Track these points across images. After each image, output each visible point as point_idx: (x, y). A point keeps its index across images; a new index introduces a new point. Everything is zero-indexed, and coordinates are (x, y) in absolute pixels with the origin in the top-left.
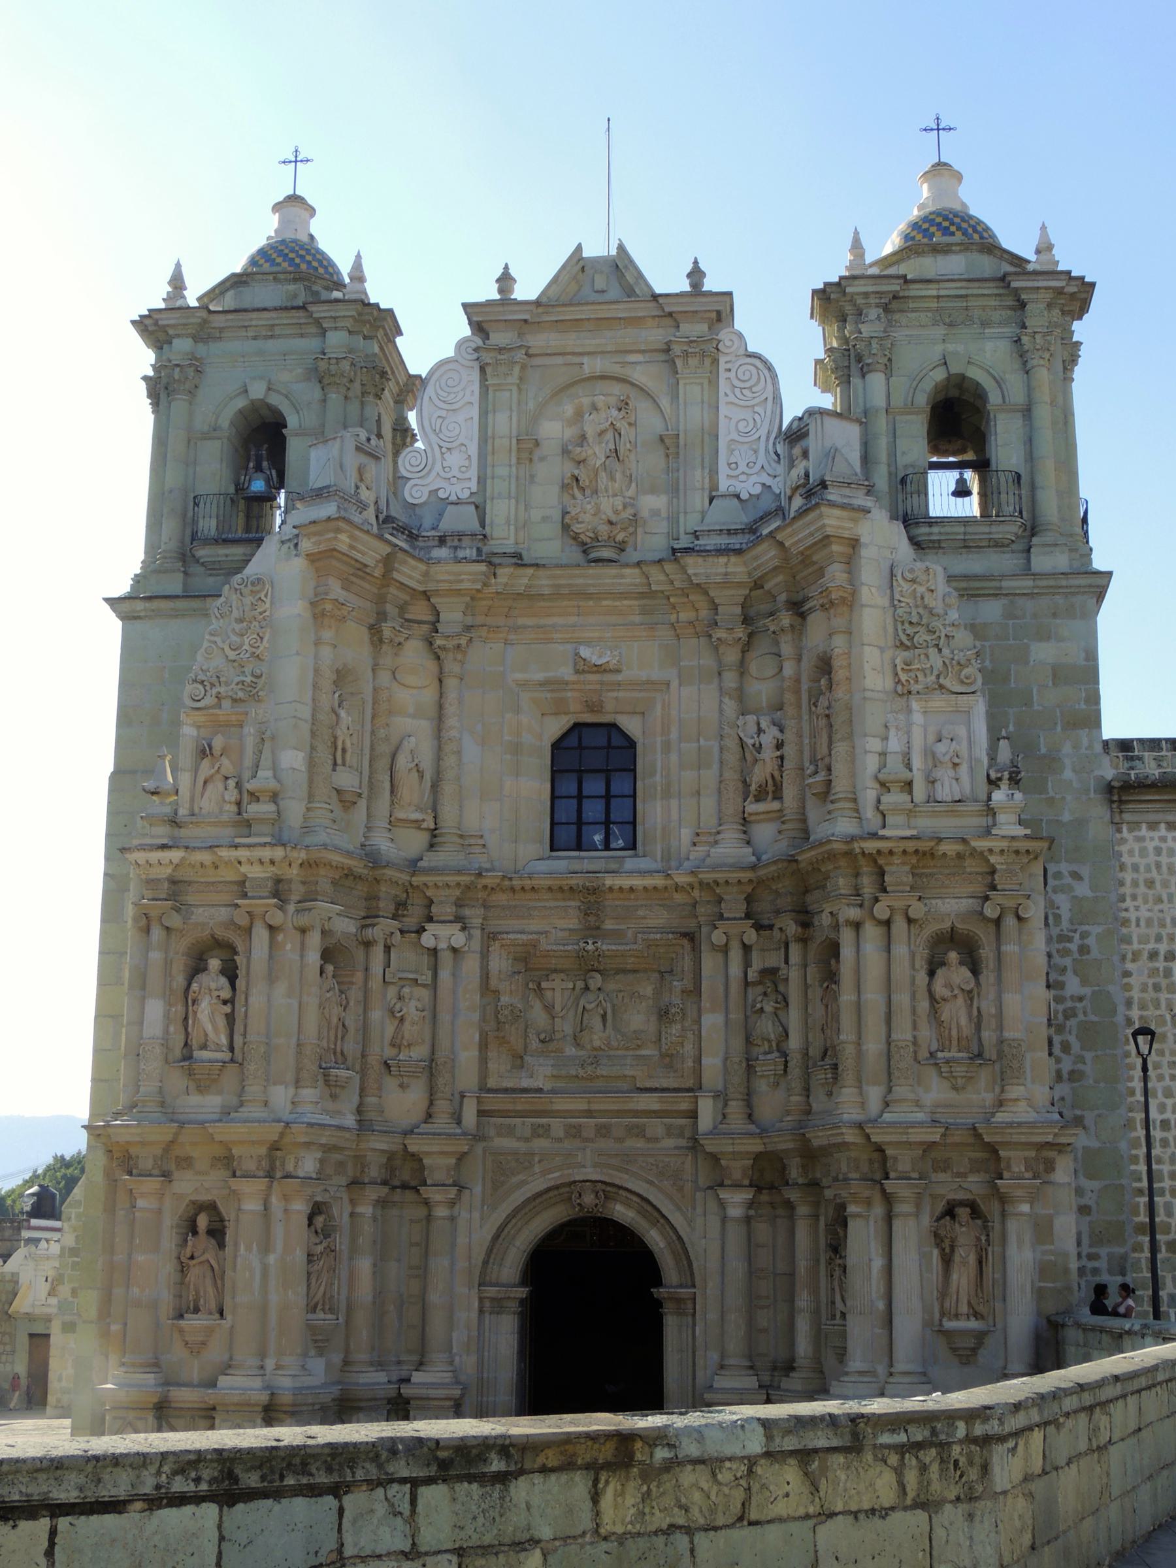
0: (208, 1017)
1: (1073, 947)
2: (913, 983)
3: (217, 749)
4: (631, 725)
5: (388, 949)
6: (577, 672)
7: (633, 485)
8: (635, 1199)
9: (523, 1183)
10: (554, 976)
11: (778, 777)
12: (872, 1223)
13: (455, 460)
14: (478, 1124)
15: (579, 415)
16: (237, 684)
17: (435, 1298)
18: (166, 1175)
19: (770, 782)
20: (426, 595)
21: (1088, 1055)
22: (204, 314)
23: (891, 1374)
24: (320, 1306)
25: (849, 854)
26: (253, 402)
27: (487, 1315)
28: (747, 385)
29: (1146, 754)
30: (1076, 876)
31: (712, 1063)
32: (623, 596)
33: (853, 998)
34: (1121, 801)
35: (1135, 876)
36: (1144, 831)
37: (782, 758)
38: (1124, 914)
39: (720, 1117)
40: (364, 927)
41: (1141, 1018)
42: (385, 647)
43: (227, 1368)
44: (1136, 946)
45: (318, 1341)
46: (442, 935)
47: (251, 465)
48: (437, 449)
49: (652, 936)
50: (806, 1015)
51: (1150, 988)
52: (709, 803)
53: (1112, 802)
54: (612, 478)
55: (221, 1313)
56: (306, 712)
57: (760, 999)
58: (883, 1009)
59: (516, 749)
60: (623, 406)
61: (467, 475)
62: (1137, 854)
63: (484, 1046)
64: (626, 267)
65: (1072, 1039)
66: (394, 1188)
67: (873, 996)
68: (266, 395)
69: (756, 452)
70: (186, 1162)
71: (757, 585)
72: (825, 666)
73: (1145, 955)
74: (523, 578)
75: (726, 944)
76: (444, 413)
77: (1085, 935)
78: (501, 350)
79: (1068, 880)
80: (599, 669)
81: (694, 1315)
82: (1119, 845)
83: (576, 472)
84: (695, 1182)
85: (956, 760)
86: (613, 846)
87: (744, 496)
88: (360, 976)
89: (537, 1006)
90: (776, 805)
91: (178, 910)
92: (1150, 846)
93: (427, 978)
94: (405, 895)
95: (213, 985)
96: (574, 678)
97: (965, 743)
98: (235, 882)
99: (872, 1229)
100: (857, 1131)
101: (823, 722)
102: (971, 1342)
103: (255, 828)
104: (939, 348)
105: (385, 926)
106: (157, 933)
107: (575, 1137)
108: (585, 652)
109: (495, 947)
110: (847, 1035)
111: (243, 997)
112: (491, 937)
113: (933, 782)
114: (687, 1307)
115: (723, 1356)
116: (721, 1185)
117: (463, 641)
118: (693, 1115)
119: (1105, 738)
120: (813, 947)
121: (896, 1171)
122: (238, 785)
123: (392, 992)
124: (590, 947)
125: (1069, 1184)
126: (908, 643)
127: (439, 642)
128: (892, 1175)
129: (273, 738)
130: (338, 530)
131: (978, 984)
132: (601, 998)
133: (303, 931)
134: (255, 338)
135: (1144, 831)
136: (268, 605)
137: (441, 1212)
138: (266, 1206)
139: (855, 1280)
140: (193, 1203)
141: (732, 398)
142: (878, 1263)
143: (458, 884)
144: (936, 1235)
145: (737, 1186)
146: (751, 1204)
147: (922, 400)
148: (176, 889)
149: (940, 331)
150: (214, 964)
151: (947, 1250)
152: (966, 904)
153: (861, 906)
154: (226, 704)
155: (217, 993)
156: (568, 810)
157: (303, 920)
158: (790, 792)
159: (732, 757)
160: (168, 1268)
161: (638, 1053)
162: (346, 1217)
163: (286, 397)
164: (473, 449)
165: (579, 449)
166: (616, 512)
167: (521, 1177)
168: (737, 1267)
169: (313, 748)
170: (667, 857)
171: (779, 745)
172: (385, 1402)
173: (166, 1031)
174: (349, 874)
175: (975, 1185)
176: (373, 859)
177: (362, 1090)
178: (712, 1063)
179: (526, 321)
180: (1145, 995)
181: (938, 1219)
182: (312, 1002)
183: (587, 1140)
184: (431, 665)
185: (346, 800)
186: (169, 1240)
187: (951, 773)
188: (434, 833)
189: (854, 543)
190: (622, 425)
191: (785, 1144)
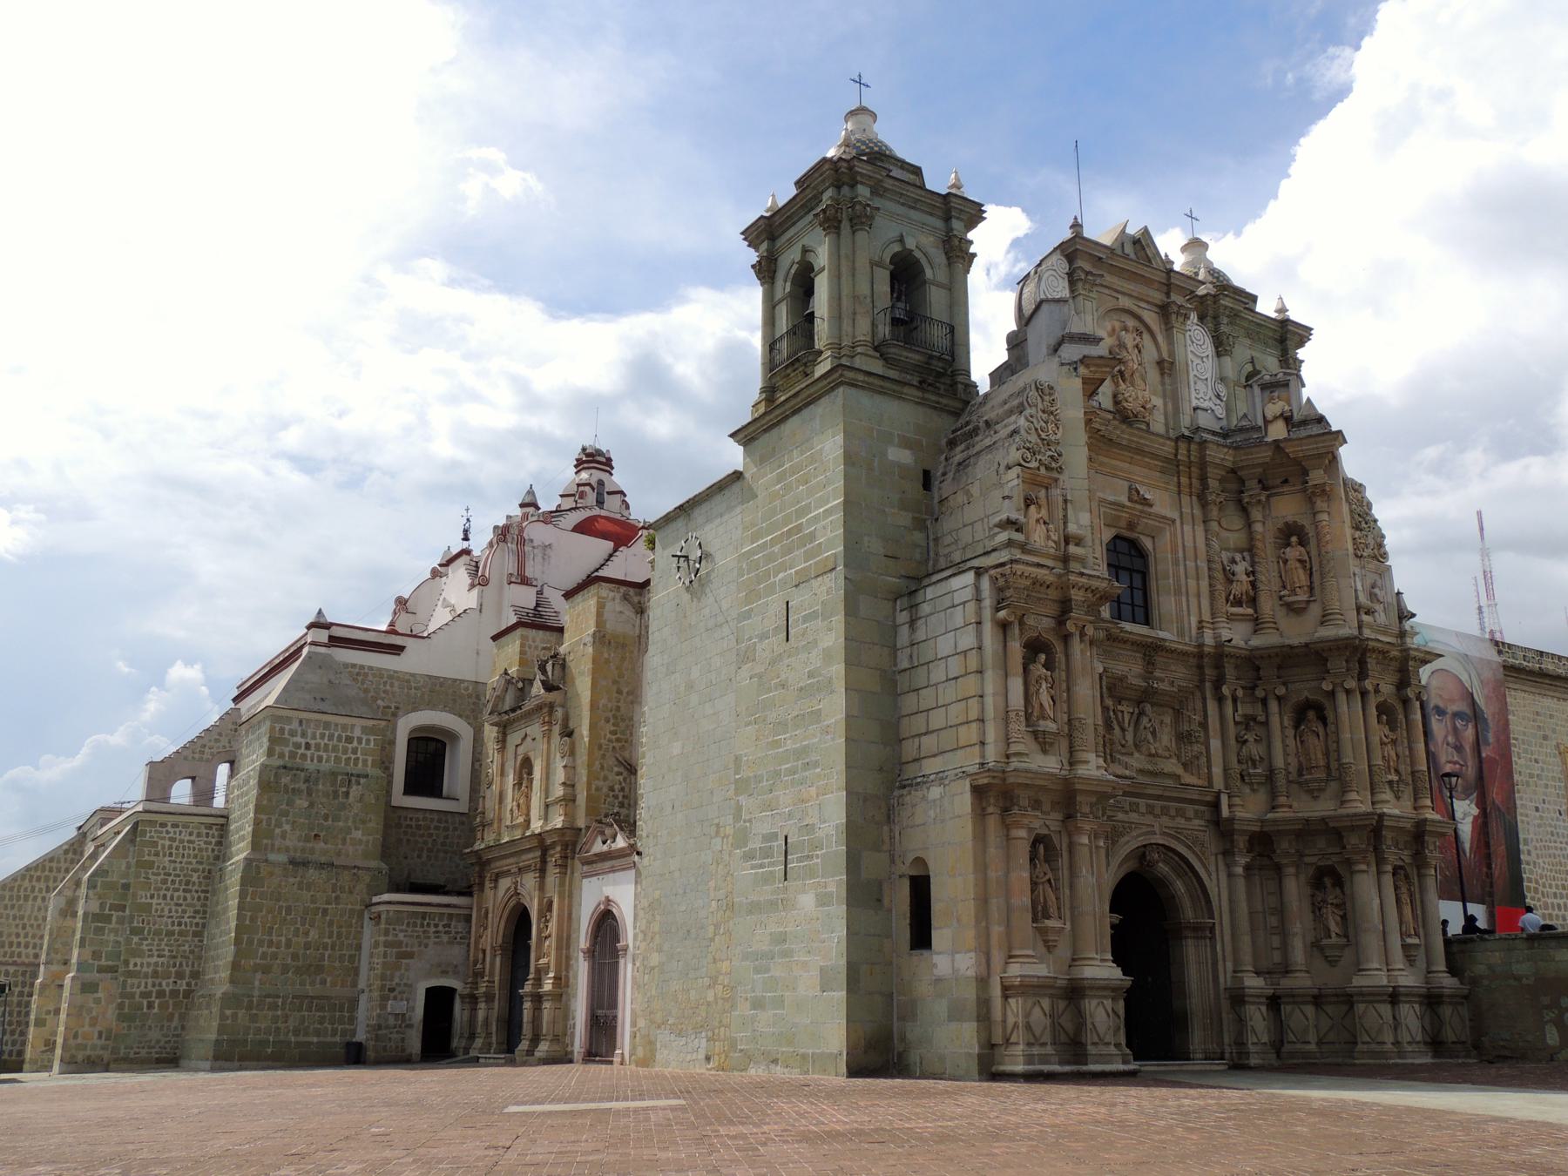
4: (1147, 543)
6: (1130, 500)
25: (1356, 648)
26: (905, 249)
31: (1217, 771)
32: (1154, 456)
50: (1285, 746)
71: (1233, 471)
78: (1087, 273)
80: (1145, 502)
81: (1212, 938)
90: (1250, 611)
104: (1248, 353)
110: (1347, 758)
114: (1206, 932)
115: (1236, 961)
146: (1247, 868)
150: (1043, 657)
154: (1043, 470)
158: (1267, 605)
159: (1219, 575)
168: (1243, 907)
178: (1217, 771)
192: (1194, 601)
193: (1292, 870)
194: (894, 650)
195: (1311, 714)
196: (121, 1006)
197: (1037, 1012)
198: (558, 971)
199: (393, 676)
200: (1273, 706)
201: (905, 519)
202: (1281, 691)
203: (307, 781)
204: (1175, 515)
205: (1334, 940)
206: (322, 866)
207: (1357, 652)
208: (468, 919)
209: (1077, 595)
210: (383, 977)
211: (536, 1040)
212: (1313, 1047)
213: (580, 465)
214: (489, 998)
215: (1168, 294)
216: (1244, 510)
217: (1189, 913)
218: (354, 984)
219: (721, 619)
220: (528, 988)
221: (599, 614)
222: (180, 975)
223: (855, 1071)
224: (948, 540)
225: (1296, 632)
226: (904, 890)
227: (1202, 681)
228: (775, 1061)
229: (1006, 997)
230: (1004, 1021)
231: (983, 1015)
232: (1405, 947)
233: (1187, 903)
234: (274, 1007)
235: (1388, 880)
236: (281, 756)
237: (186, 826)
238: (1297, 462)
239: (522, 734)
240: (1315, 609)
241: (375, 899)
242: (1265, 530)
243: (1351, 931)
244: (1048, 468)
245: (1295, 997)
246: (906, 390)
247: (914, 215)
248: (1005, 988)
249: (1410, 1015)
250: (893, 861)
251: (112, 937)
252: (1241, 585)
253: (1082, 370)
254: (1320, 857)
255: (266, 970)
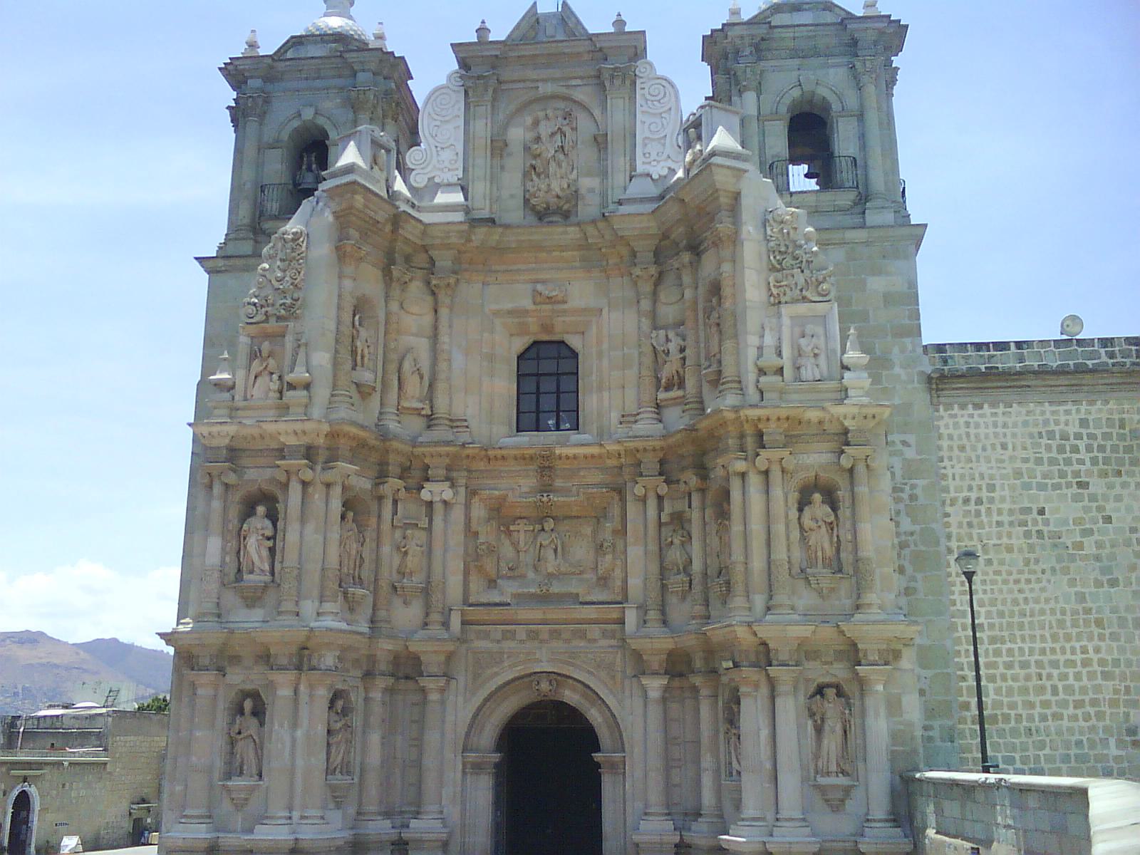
0: (255, 549)
1: (905, 496)
2: (787, 516)
3: (265, 354)
4: (574, 342)
5: (395, 502)
6: (535, 303)
7: (575, 171)
8: (579, 685)
9: (496, 674)
10: (519, 521)
11: (682, 373)
12: (759, 702)
13: (447, 155)
14: (463, 631)
15: (536, 123)
16: (281, 305)
17: (429, 762)
18: (221, 670)
19: (676, 378)
20: (425, 249)
21: (919, 576)
22: (270, 61)
23: (777, 820)
24: (338, 770)
27: (469, 776)
28: (658, 98)
29: (956, 354)
30: (904, 443)
31: (635, 583)
33: (741, 528)
34: (937, 390)
35: (950, 443)
36: (956, 410)
37: (684, 359)
38: (943, 471)
39: (642, 622)
40: (377, 484)
41: (958, 547)
42: (394, 284)
43: (262, 819)
44: (953, 494)
45: (337, 798)
46: (436, 491)
47: (304, 167)
48: (434, 148)
49: (590, 491)
50: (705, 545)
51: (965, 525)
52: (631, 394)
53: (933, 389)
54: (560, 166)
55: (260, 775)
56: (332, 326)
57: (670, 534)
58: (763, 537)
59: (491, 358)
60: (567, 116)
61: (454, 167)
62: (951, 426)
63: (466, 573)
64: (568, 18)
65: (906, 564)
66: (398, 679)
67: (756, 526)
68: (314, 118)
69: (664, 145)
70: (235, 659)
71: (665, 236)
72: (716, 289)
73: (960, 501)
74: (495, 235)
75: (645, 495)
76: (438, 123)
77: (913, 487)
79: (900, 447)
82: (938, 420)
83: (534, 162)
84: (624, 672)
85: (816, 351)
86: (562, 428)
87: (655, 176)
88: (373, 521)
89: (507, 542)
90: (680, 393)
91: (235, 471)
92: (962, 421)
93: (424, 523)
94: (409, 463)
95: (259, 526)
96: (533, 307)
97: (822, 338)
98: (277, 449)
99: (759, 707)
100: (746, 629)
101: (714, 329)
102: (840, 795)
103: (291, 410)
105: (394, 483)
106: (217, 489)
107: (534, 639)
108: (539, 287)
109: (476, 500)
110: (738, 556)
111: (282, 534)
112: (472, 493)
113: (799, 368)
114: (618, 768)
115: (646, 806)
116: (644, 673)
117: (452, 281)
118: (621, 622)
119: (924, 343)
120: (710, 495)
121: (777, 660)
122: (280, 378)
123: (398, 534)
124: (545, 499)
125: (913, 670)
126: (778, 266)
127: (434, 282)
128: (774, 662)
129: (306, 345)
130: (354, 192)
131: (836, 516)
132: (553, 536)
133: (328, 485)
134: (307, 79)
135: (956, 410)
136: (304, 249)
137: (434, 697)
138: (296, 691)
139: (747, 745)
140: (242, 691)
141: (643, 109)
142: (765, 733)
143: (448, 455)
144: (809, 709)
145: (655, 673)
146: (667, 689)
147: (783, 109)
148: (234, 454)
149: (797, 62)
150: (261, 510)
151: (819, 722)
152: (826, 458)
153: (745, 459)
155: (261, 532)
156: (529, 402)
157: (329, 476)
158: (690, 383)
159: (648, 360)
160: (221, 743)
161: (579, 576)
162: (361, 701)
163: (329, 118)
164: (460, 148)
165: (536, 146)
166: (562, 189)
167: (495, 669)
168: (656, 737)
169: (337, 351)
170: (600, 434)
171: (682, 350)
172: (388, 844)
173: (223, 563)
174: (363, 444)
175: (838, 672)
176: (385, 436)
177: (374, 605)
179: (496, 56)
180: (961, 531)
181: (812, 696)
182: (334, 536)
183: (541, 641)
184: (429, 299)
185: (363, 391)
186: (222, 720)
187: (812, 360)
188: (430, 418)
189: (737, 196)
190: (567, 129)
191: (690, 642)
235: (789, 708)
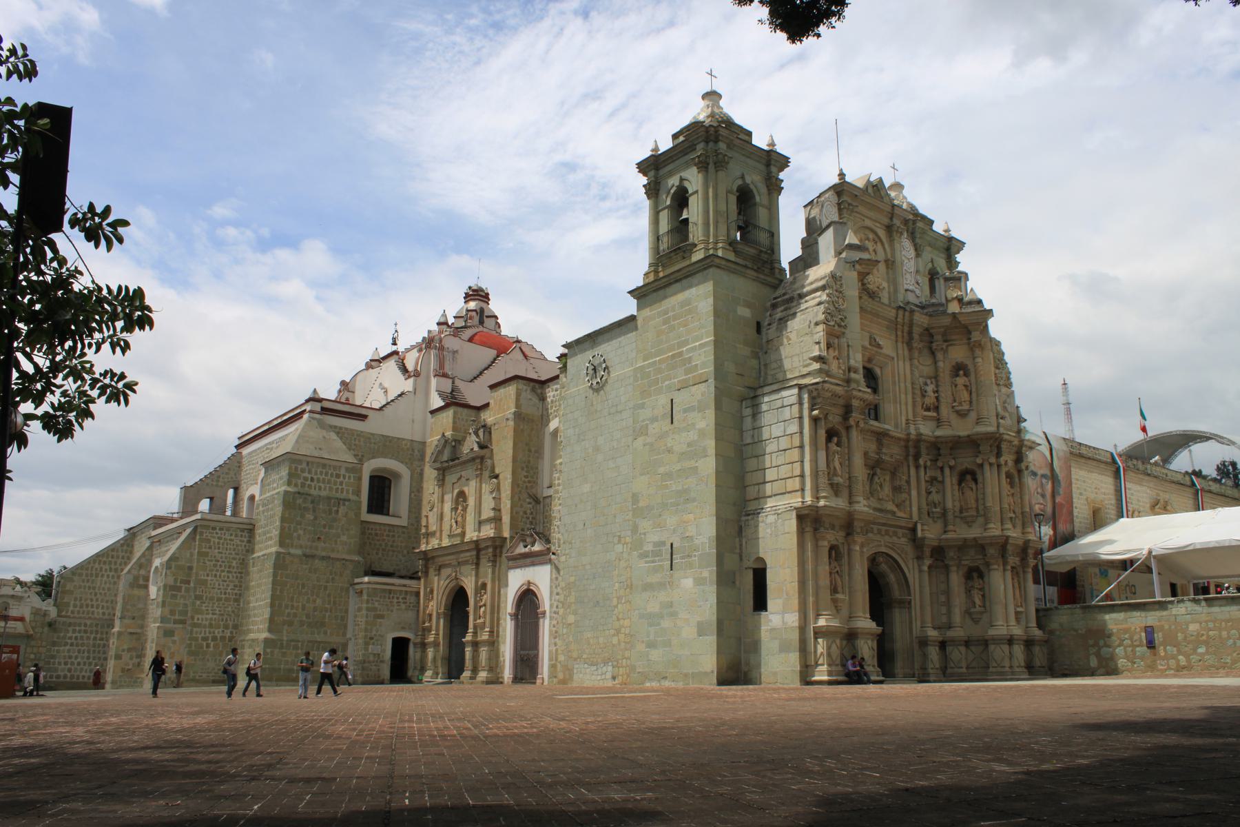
4: (878, 371)
50: (953, 495)
71: (927, 330)
80: (879, 346)
81: (910, 608)
115: (923, 622)
158: (945, 411)
159: (918, 392)
168: (927, 590)
178: (915, 509)
192: (903, 407)
193: (954, 569)
194: (742, 432)
195: (969, 477)
196: (190, 646)
197: (834, 646)
198: (492, 627)
199: (360, 434)
200: (947, 471)
201: (745, 351)
202: (952, 463)
203: (312, 502)
204: (894, 355)
205: (978, 609)
206: (323, 558)
207: (995, 442)
208: (418, 594)
209: (855, 403)
210: (366, 630)
211: (475, 671)
212: (964, 670)
213: (468, 298)
214: (436, 644)
215: (891, 219)
216: (933, 353)
217: (897, 593)
218: (344, 634)
219: (620, 408)
220: (469, 637)
221: (518, 400)
222: (226, 627)
223: (721, 682)
224: (774, 365)
225: (962, 429)
226: (749, 578)
227: (908, 455)
228: (665, 678)
229: (816, 638)
230: (815, 651)
231: (803, 649)
232: (1017, 613)
233: (896, 586)
234: (296, 648)
235: (1009, 574)
236: (296, 485)
237: (228, 529)
238: (965, 327)
239: (458, 475)
240: (973, 415)
241: (357, 580)
242: (945, 366)
243: (987, 604)
244: (839, 326)
245: (954, 642)
246: (749, 271)
247: (749, 161)
248: (815, 633)
249: (1018, 650)
250: (741, 560)
251: (182, 601)
252: (930, 400)
253: (857, 266)
254: (974, 563)
255: (290, 624)
